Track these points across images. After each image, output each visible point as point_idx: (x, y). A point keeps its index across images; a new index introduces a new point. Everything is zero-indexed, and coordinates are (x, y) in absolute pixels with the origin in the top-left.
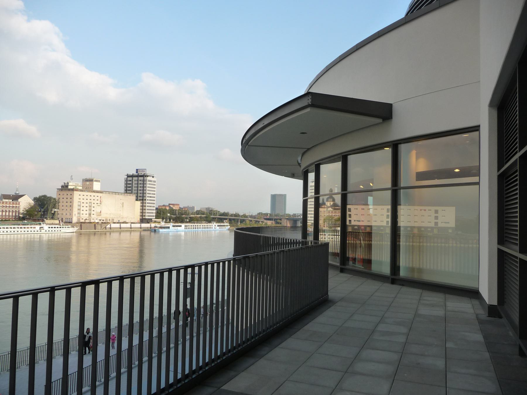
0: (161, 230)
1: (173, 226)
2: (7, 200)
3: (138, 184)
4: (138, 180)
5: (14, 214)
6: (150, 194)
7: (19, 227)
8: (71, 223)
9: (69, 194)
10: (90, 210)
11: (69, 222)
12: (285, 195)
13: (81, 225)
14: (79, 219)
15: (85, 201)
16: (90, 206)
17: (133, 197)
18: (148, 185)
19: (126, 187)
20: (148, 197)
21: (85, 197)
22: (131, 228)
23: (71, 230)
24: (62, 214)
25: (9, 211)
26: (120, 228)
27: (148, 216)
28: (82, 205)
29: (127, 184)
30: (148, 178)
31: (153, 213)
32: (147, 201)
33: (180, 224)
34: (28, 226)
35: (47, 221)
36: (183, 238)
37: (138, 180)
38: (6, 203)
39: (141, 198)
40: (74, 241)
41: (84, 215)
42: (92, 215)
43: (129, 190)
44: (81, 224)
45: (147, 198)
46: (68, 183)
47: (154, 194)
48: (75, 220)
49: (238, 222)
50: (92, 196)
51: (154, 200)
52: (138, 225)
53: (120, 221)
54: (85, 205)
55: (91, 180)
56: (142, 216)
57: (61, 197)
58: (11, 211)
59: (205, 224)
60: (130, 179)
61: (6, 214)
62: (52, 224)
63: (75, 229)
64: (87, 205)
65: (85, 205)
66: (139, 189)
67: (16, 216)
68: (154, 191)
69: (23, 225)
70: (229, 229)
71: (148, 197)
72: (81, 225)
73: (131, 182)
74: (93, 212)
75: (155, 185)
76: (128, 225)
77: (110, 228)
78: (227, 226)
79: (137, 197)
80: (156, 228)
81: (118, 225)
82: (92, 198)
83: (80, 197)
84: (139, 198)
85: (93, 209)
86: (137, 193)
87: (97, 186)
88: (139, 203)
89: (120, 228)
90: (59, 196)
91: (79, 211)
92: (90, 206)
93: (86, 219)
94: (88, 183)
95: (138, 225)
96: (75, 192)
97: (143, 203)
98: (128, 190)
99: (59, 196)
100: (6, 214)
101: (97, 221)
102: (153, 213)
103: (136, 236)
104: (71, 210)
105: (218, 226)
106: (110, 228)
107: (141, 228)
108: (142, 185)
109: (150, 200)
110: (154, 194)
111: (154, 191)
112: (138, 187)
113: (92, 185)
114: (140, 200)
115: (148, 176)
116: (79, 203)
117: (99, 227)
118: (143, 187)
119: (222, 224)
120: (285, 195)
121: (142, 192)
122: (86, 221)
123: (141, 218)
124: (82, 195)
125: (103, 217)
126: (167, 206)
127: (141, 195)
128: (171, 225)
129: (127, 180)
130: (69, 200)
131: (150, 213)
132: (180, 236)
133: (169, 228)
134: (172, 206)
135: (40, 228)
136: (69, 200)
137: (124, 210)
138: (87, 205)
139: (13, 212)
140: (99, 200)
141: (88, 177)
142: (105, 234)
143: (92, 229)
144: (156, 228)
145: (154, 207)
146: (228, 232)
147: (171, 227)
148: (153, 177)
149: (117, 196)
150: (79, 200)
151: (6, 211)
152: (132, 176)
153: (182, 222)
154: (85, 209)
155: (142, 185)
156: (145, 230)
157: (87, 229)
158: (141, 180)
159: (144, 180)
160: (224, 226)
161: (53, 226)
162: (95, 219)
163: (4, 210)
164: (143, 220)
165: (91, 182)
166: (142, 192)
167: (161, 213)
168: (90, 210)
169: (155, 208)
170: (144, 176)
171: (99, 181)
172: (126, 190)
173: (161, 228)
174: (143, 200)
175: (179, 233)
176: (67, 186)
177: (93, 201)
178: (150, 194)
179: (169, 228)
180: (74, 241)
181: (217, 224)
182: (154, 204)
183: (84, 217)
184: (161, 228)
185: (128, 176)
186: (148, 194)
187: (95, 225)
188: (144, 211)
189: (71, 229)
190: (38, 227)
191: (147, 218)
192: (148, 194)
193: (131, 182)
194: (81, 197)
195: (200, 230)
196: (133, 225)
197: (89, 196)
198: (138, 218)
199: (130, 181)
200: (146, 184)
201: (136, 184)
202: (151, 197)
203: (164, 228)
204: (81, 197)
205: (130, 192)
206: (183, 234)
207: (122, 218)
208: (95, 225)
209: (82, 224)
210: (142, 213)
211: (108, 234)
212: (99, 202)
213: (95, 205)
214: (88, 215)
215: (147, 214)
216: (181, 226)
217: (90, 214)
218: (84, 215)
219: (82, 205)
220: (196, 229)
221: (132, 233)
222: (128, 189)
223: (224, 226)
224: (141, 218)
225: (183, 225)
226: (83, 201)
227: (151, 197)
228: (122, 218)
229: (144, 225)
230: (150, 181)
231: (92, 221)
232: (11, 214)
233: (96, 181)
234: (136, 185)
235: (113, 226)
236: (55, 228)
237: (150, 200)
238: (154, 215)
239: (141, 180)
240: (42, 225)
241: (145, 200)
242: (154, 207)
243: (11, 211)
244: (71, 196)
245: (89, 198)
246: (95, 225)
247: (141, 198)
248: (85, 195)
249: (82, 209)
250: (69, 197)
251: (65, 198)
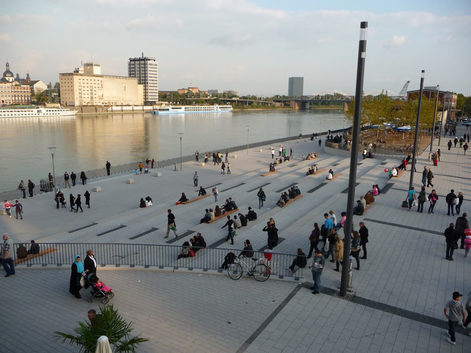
0: (160, 112)
1: (173, 108)
2: (25, 86)
3: (140, 68)
4: (140, 64)
5: (26, 99)
6: (152, 77)
7: (17, 110)
8: (74, 106)
9: (70, 79)
10: (92, 94)
11: (72, 106)
13: (82, 109)
14: (81, 103)
16: (92, 90)
17: (135, 81)
18: (149, 69)
19: (130, 71)
20: (150, 80)
21: (85, 81)
22: (133, 110)
23: (70, 113)
24: (66, 98)
25: (18, 96)
26: (122, 111)
27: (151, 99)
28: (83, 89)
29: (130, 68)
30: (149, 62)
31: (156, 96)
32: (149, 85)
33: (180, 106)
34: (18, 110)
35: (47, 105)
36: (183, 119)
37: (140, 64)
38: (24, 88)
39: (143, 81)
40: (78, 123)
41: (86, 98)
42: (94, 99)
43: (133, 74)
44: (82, 107)
45: (149, 82)
46: (78, 69)
47: (156, 78)
48: (77, 103)
49: (246, 104)
50: (93, 80)
51: (157, 84)
52: (141, 108)
53: (123, 104)
54: (86, 89)
55: (91, 65)
56: (145, 99)
57: (63, 81)
58: (23, 95)
59: (207, 106)
60: (133, 63)
61: (18, 98)
62: (54, 107)
63: (75, 112)
64: (89, 89)
65: (86, 89)
66: (141, 72)
67: (28, 100)
69: (21, 108)
70: (231, 111)
71: (150, 80)
72: (82, 109)
73: (133, 66)
74: (94, 96)
76: (130, 108)
77: (112, 111)
78: (230, 108)
79: (140, 80)
80: (156, 111)
81: (119, 108)
82: (93, 82)
83: (80, 81)
84: (142, 82)
85: (94, 93)
86: (140, 77)
87: (97, 70)
88: (141, 87)
89: (122, 111)
90: (62, 81)
91: (80, 95)
92: (92, 90)
93: (89, 103)
94: (88, 68)
95: (141, 108)
96: (74, 77)
97: (145, 86)
98: (131, 74)
99: (62, 81)
100: (18, 98)
101: (99, 104)
102: (156, 96)
103: (139, 119)
104: (73, 94)
105: (220, 108)
106: (112, 111)
107: (143, 110)
108: (143, 69)
109: (152, 83)
112: (140, 71)
113: (92, 69)
114: (143, 83)
115: (149, 60)
116: (80, 88)
117: (101, 110)
118: (145, 71)
119: (225, 106)
121: (144, 75)
122: (89, 104)
123: (145, 100)
124: (96, 80)
125: (106, 100)
126: (186, 89)
127: (144, 78)
128: (170, 107)
129: (130, 65)
130: (70, 85)
131: (153, 96)
132: (181, 117)
133: (168, 110)
134: (191, 90)
135: (38, 111)
136: (70, 85)
137: (130, 94)
138: (89, 89)
139: (25, 96)
140: (100, 84)
141: (89, 61)
142: (107, 116)
143: (94, 112)
144: (156, 111)
145: (157, 90)
146: (232, 113)
147: (171, 110)
148: (154, 60)
149: (119, 80)
150: (80, 84)
151: (18, 96)
152: (135, 60)
153: (183, 104)
154: (86, 92)
155: (143, 69)
156: (148, 112)
157: (88, 112)
159: (145, 64)
160: (227, 108)
161: (54, 109)
162: (97, 102)
163: (16, 95)
164: (146, 103)
165: (91, 67)
166: (144, 75)
167: (164, 96)
168: (92, 94)
169: (157, 91)
170: (145, 59)
172: (130, 74)
173: (160, 110)
174: (145, 83)
175: (179, 115)
176: (78, 72)
177: (94, 86)
178: (152, 77)
179: (168, 110)
180: (78, 123)
181: (219, 106)
182: (157, 87)
183: (86, 100)
184: (160, 110)
185: (131, 60)
186: (150, 77)
187: (96, 108)
188: (147, 94)
189: (69, 112)
190: (35, 111)
191: (149, 100)
192: (150, 77)
193: (133, 66)
194: (82, 81)
195: (201, 111)
196: (135, 108)
197: (89, 80)
198: (142, 101)
199: (133, 65)
200: (147, 67)
201: (138, 68)
202: (153, 80)
203: (163, 110)
204: (82, 81)
205: (134, 76)
206: (183, 115)
207: (125, 101)
208: (96, 108)
209: (83, 107)
210: (145, 96)
211: (110, 117)
212: (100, 86)
213: (97, 89)
214: (90, 99)
215: (149, 97)
216: (181, 108)
217: (92, 98)
218: (86, 98)
219: (83, 89)
220: (208, 111)
221: (135, 116)
222: (132, 73)
223: (227, 108)
224: (145, 100)
225: (183, 107)
226: (84, 85)
227: (153, 80)
228: (125, 101)
229: (146, 108)
230: (151, 64)
231: (95, 104)
232: (23, 98)
234: (139, 69)
235: (115, 108)
236: (53, 111)
237: (152, 83)
238: (158, 97)
239: (142, 64)
240: (40, 109)
241: (147, 83)
242: (157, 90)
243: (23, 95)
245: (89, 82)
246: (96, 108)
247: (144, 82)
248: (96, 80)
249: (83, 92)
250: (70, 81)
251: (67, 83)
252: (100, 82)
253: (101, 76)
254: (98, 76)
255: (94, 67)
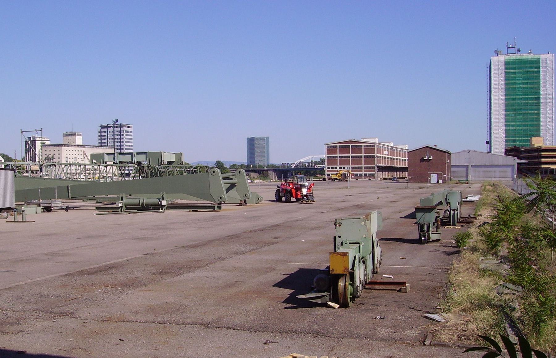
6: (128, 146)
12: (268, 138)
15: (71, 156)
47: (132, 146)
60: (105, 130)
68: (132, 142)
75: (132, 136)
94: (70, 137)
96: (63, 148)
110: (132, 146)
111: (132, 142)
112: (114, 139)
120: (268, 138)
150: (67, 156)
152: (107, 127)
158: (117, 131)
159: (120, 132)
165: (73, 137)
171: (80, 135)
178: (128, 146)
185: (102, 127)
193: (106, 134)
199: (104, 132)
233: (78, 135)
239: (117, 131)
244: (59, 152)
252: (82, 153)
253: (83, 146)
254: (81, 146)
255: (77, 137)
